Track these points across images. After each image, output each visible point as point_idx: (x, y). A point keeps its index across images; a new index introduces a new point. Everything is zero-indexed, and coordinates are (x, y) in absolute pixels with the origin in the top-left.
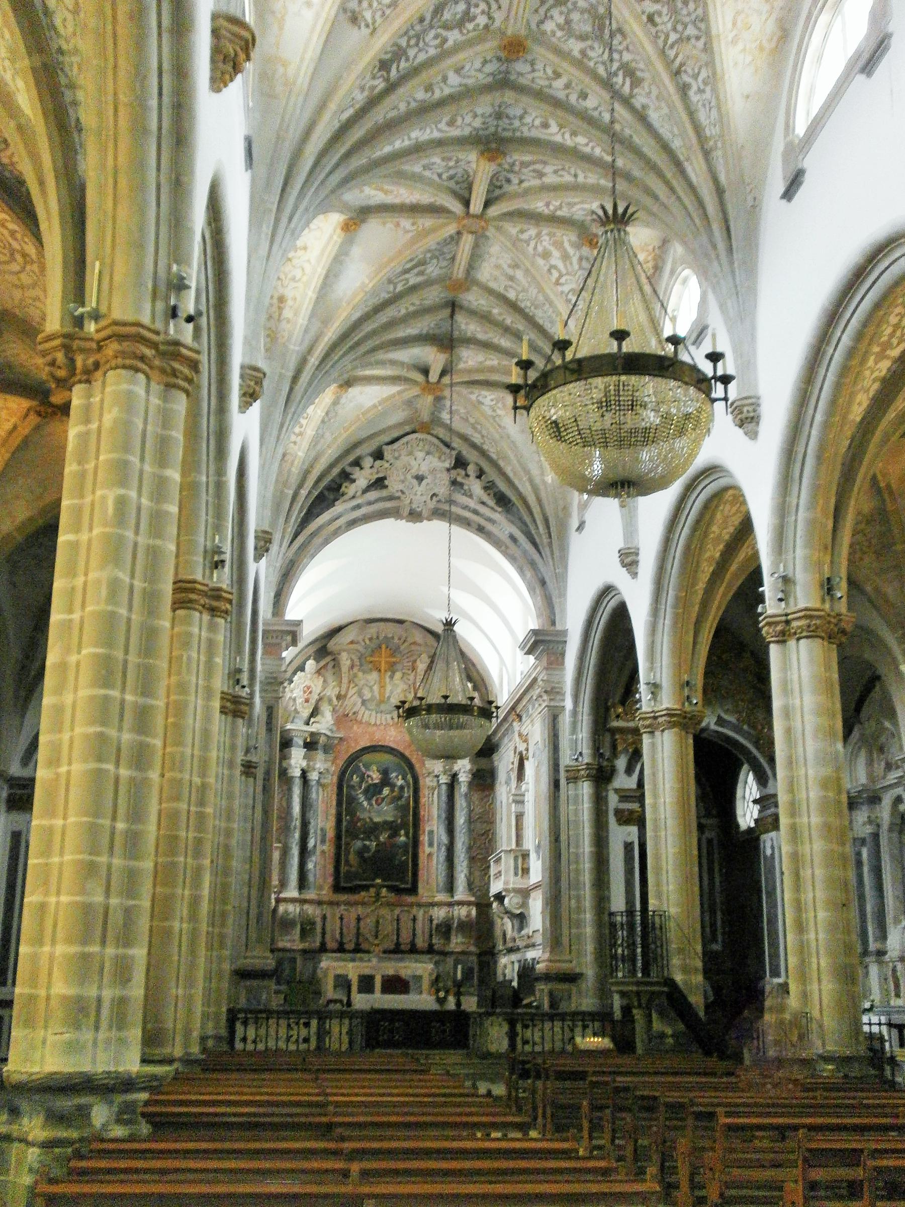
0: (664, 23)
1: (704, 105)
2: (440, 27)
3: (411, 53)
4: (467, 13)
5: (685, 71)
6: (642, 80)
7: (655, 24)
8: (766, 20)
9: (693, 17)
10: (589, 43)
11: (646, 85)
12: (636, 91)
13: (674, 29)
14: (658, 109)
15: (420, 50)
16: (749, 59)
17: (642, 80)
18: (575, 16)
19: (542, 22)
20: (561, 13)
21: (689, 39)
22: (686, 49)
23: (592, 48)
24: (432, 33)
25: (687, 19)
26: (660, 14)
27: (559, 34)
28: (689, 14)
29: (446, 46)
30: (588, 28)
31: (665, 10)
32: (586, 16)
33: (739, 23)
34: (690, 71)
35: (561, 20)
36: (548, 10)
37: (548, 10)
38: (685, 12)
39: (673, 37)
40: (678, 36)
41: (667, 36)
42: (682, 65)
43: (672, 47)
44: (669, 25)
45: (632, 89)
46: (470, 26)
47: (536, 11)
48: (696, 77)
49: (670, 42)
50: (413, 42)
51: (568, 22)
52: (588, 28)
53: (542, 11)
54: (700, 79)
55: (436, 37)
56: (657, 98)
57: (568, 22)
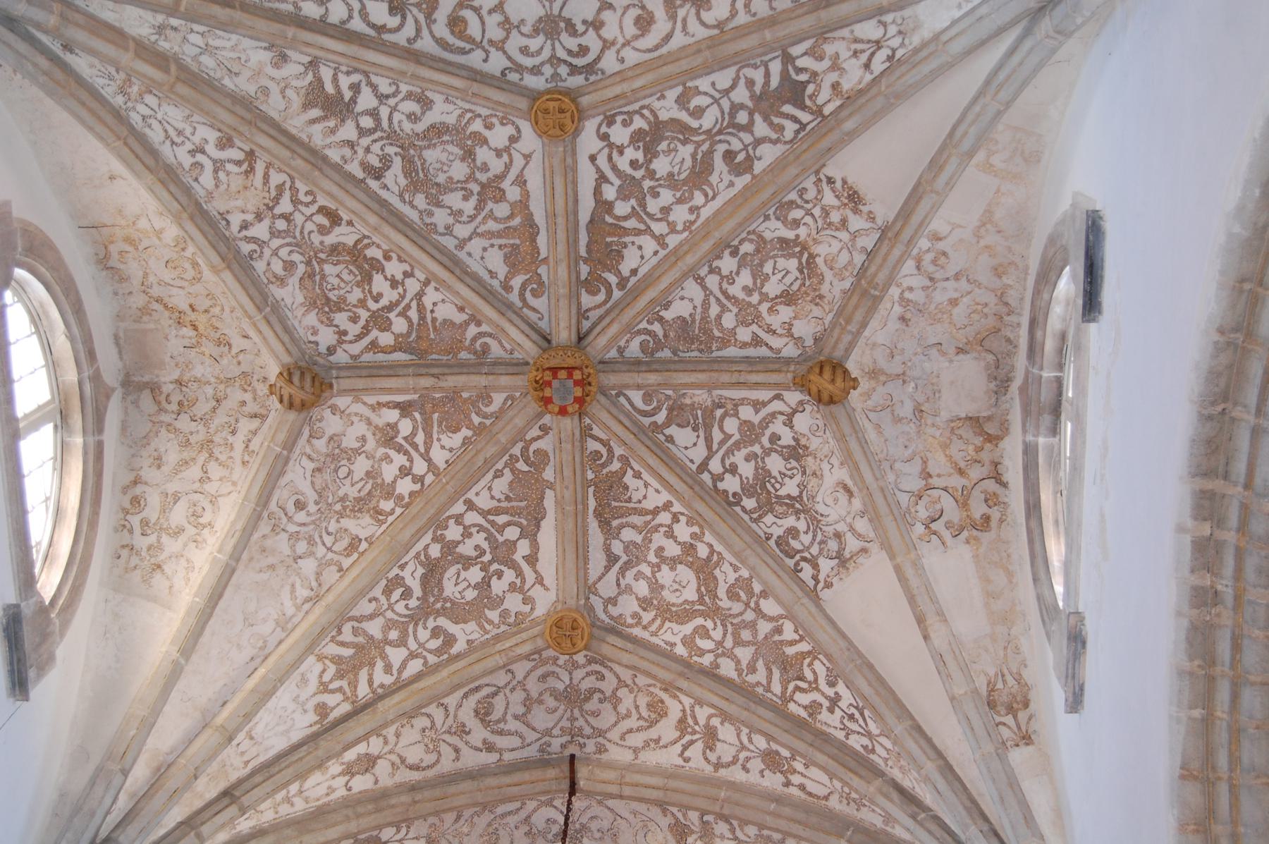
0: (309, 218)
1: (180, 133)
2: (695, 131)
3: (741, 95)
4: (651, 153)
5: (238, 163)
6: (306, 106)
7: (322, 210)
8: (146, 275)
9: (267, 252)
10: (420, 127)
11: (296, 101)
12: (310, 77)
13: (287, 217)
14: (258, 73)
15: (726, 92)
16: (143, 224)
17: (306, 106)
18: (459, 170)
19: (513, 139)
20: (485, 167)
21: (259, 217)
22: (254, 200)
23: (413, 118)
24: (707, 121)
25: (276, 243)
26: (322, 230)
27: (477, 126)
28: (275, 253)
29: (680, 89)
30: (431, 155)
31: (316, 238)
32: (441, 179)
33: (187, 265)
34: (229, 167)
35: (483, 154)
36: (508, 167)
37: (508, 167)
38: (283, 252)
39: (285, 206)
40: (278, 211)
41: (295, 202)
42: (251, 170)
43: (280, 188)
44: (299, 219)
45: (319, 81)
46: (639, 123)
47: (527, 157)
48: (218, 166)
49: (287, 195)
50: (742, 117)
51: (469, 155)
52: (431, 155)
53: (519, 162)
54: (209, 166)
55: (698, 113)
56: (265, 91)
57: (469, 155)
